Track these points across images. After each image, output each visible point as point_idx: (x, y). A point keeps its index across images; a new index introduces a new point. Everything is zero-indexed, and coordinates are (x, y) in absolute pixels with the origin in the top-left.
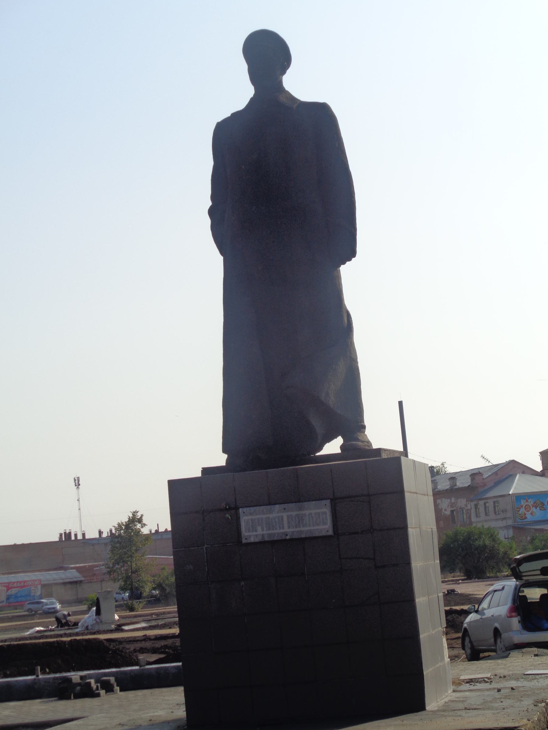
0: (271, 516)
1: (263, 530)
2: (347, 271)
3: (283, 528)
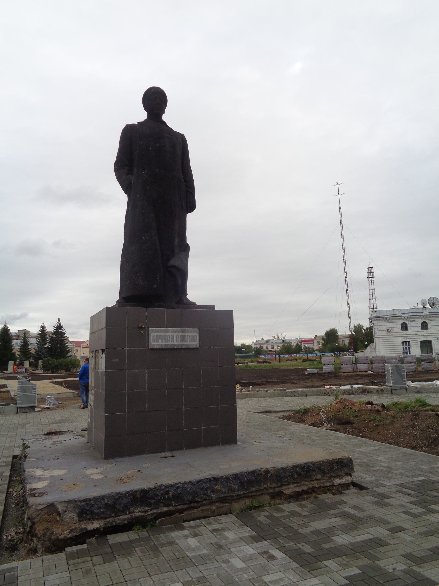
0: (167, 334)
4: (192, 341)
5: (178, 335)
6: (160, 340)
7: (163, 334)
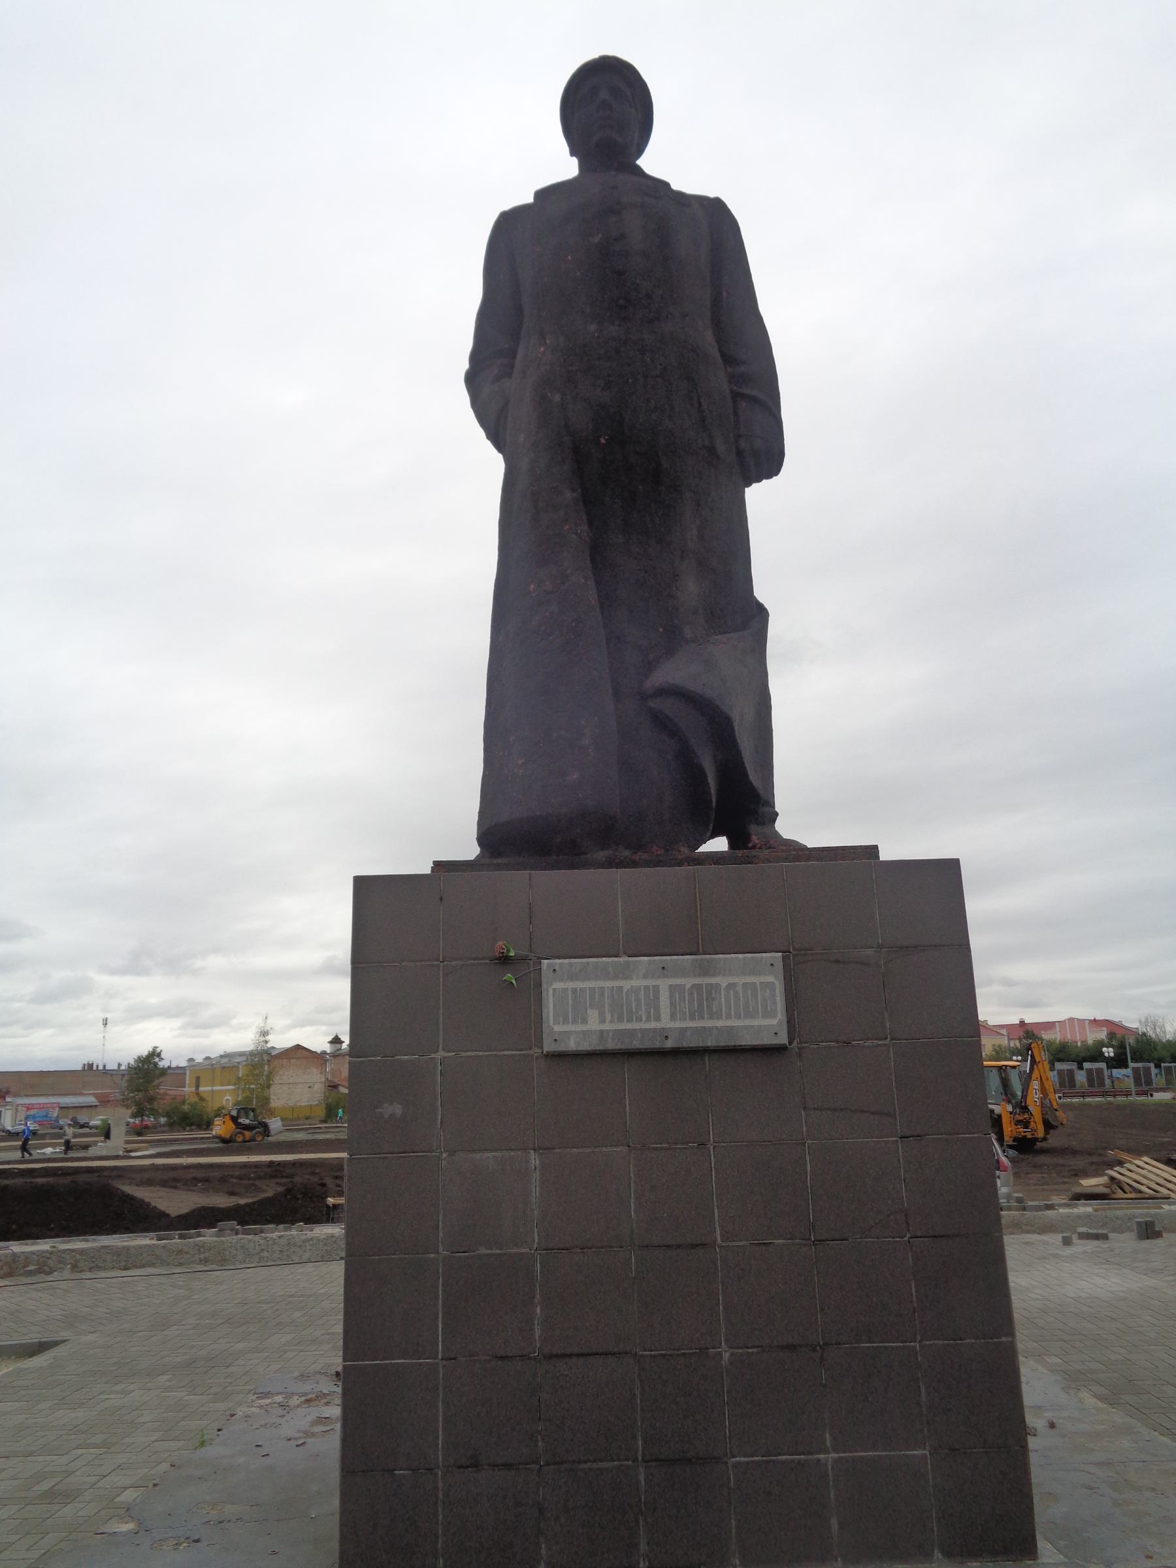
0: (627, 985)
1: (603, 1021)
2: (759, 498)
3: (658, 1018)
4: (750, 1014)
5: (681, 987)
6: (593, 1015)
7: (608, 984)
